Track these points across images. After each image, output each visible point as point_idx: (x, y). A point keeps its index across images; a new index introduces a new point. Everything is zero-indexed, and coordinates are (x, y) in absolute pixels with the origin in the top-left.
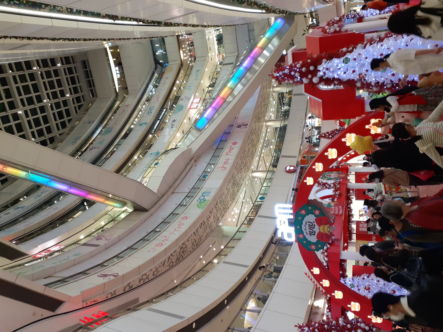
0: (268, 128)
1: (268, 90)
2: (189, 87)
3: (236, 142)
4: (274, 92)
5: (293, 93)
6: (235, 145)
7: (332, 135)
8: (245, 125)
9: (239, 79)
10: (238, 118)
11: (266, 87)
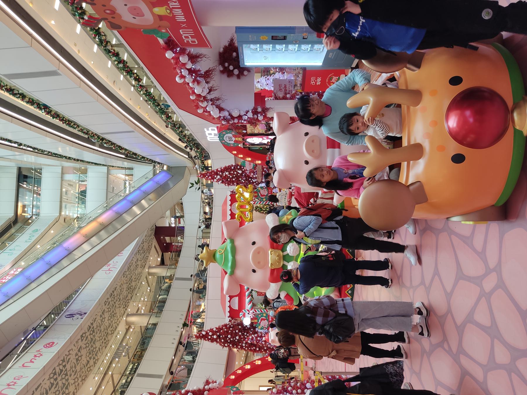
0: (130, 327)
1: (139, 270)
2: (10, 250)
3: (53, 343)
4: (150, 274)
5: (176, 276)
6: (49, 347)
7: (218, 334)
8: (82, 313)
9: (85, 237)
10: (75, 301)
11: (136, 263)
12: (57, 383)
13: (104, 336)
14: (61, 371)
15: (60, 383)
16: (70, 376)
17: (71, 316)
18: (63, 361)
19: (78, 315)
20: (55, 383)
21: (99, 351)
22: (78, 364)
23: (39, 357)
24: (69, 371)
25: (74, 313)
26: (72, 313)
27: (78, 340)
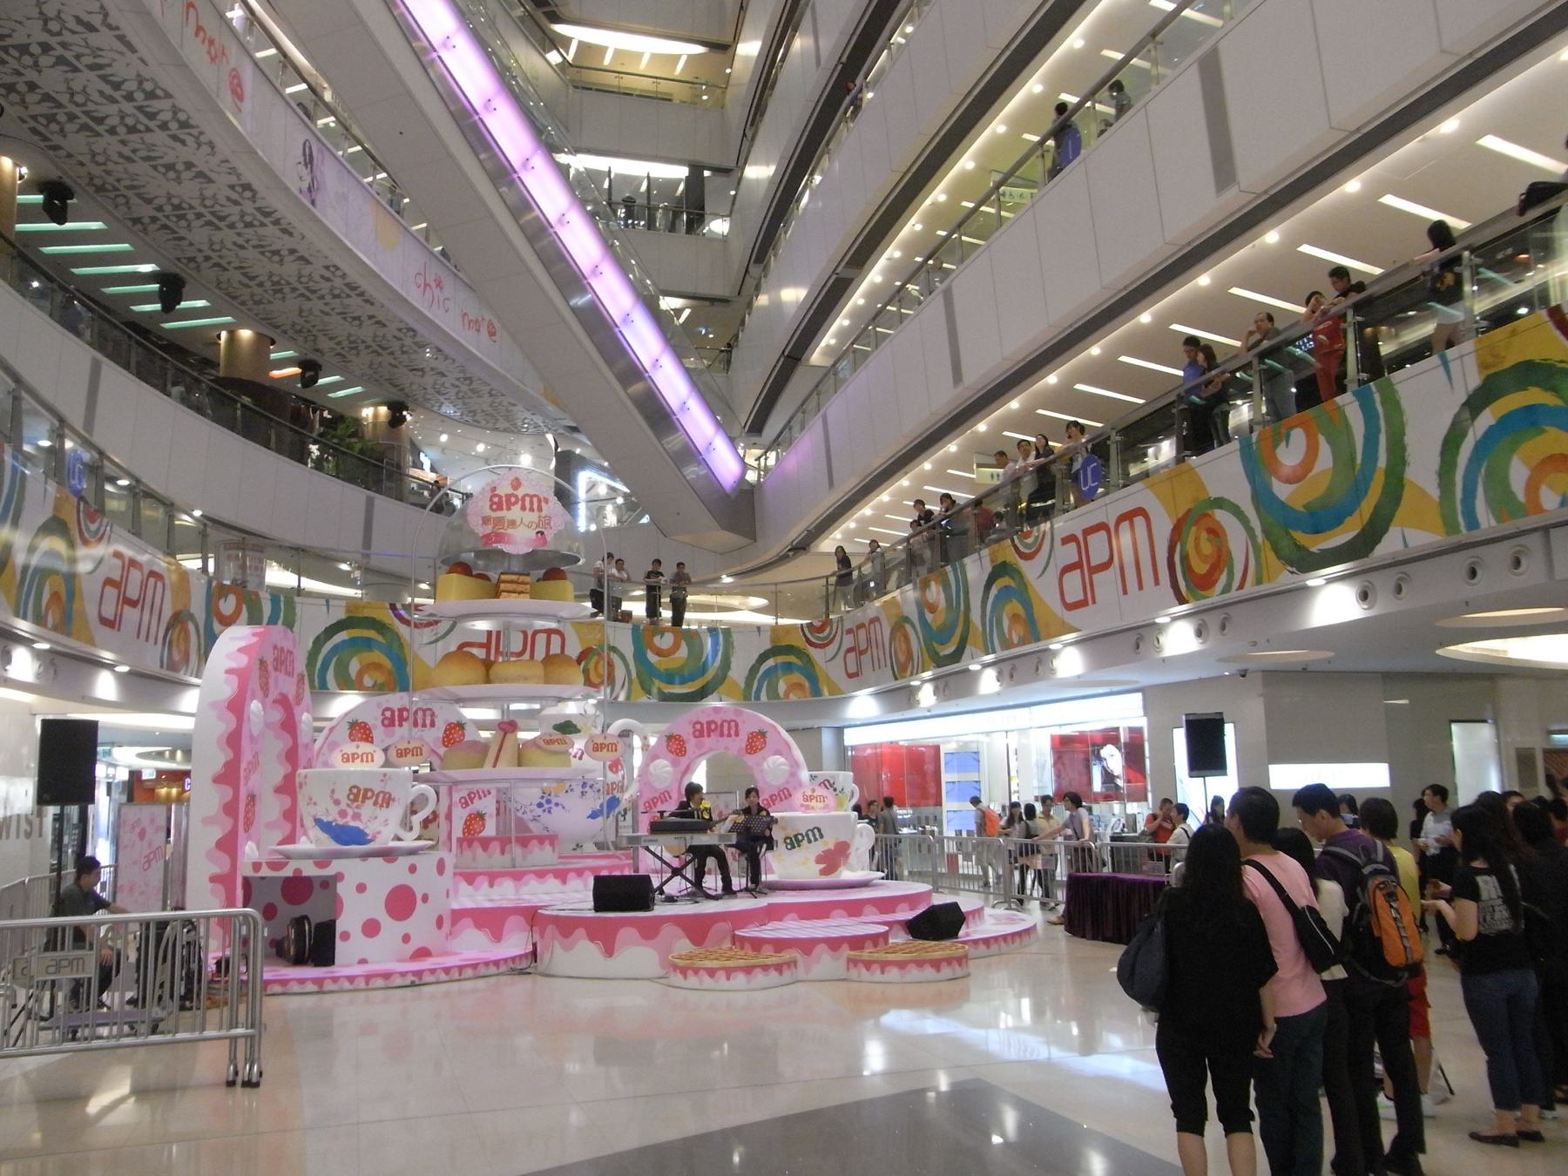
6: (231, 83)
8: (313, 194)
12: (113, 100)
13: (220, 257)
14: (152, 116)
15: (112, 109)
16: (123, 142)
17: (309, 161)
18: (184, 125)
19: (308, 180)
20: (117, 95)
21: (175, 239)
22: (155, 167)
23: (209, 52)
24: (142, 138)
25: (315, 167)
26: (315, 162)
27: (239, 176)
